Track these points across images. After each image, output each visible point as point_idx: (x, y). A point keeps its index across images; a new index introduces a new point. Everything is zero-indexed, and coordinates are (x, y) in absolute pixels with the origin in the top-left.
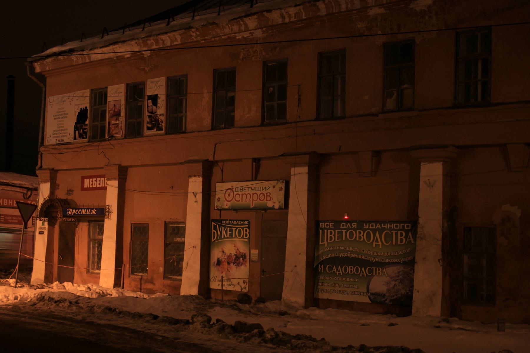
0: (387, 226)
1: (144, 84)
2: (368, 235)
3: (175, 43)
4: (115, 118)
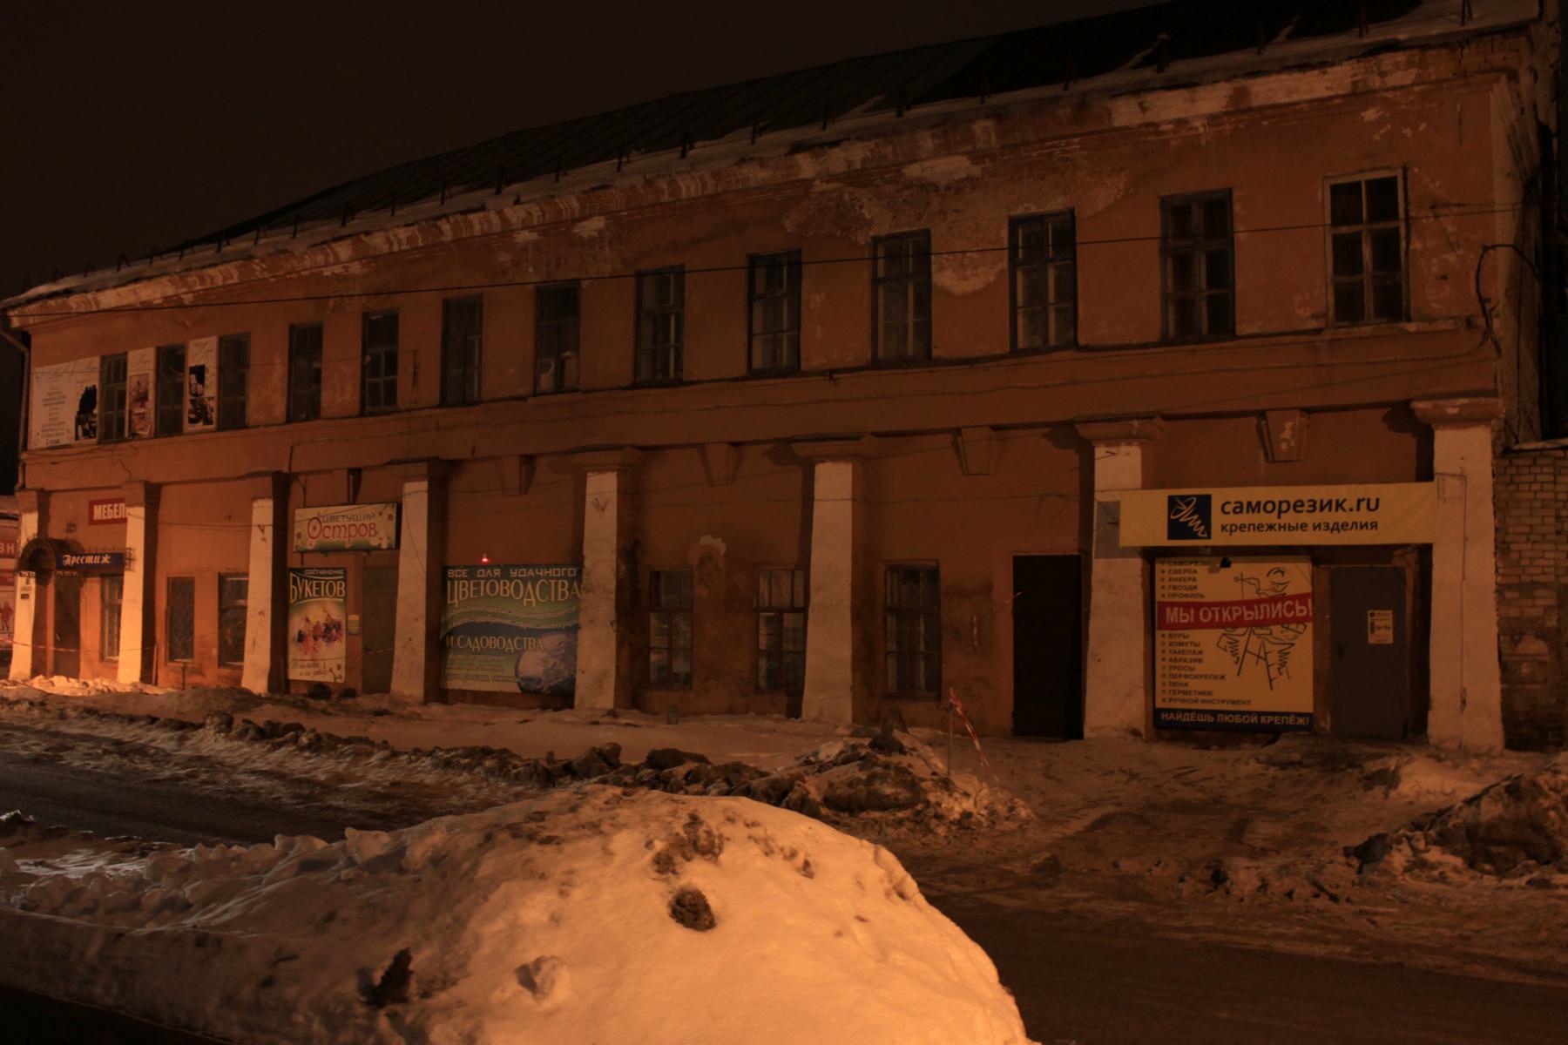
0: (543, 572)
1: (184, 347)
2: (517, 585)
3: (230, 282)
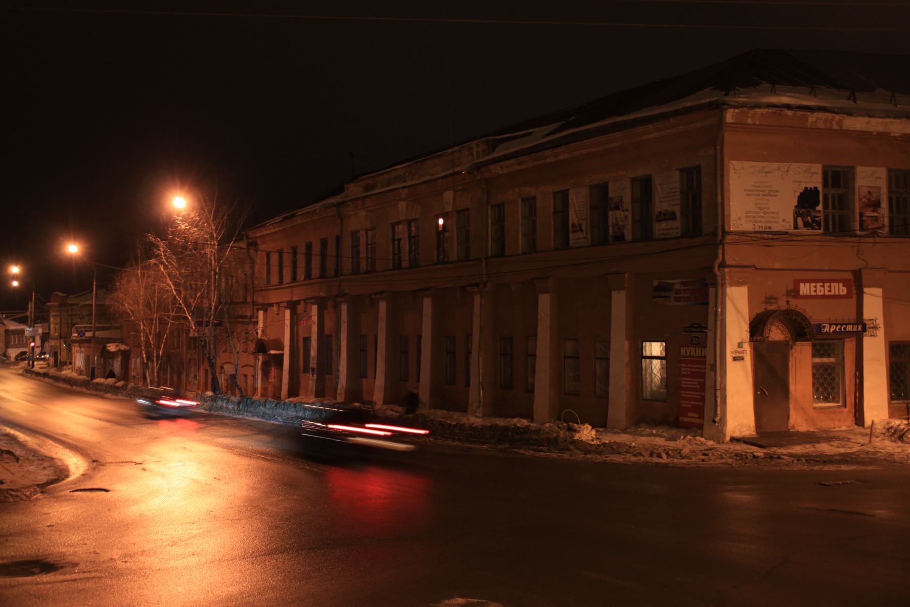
4: (872, 209)
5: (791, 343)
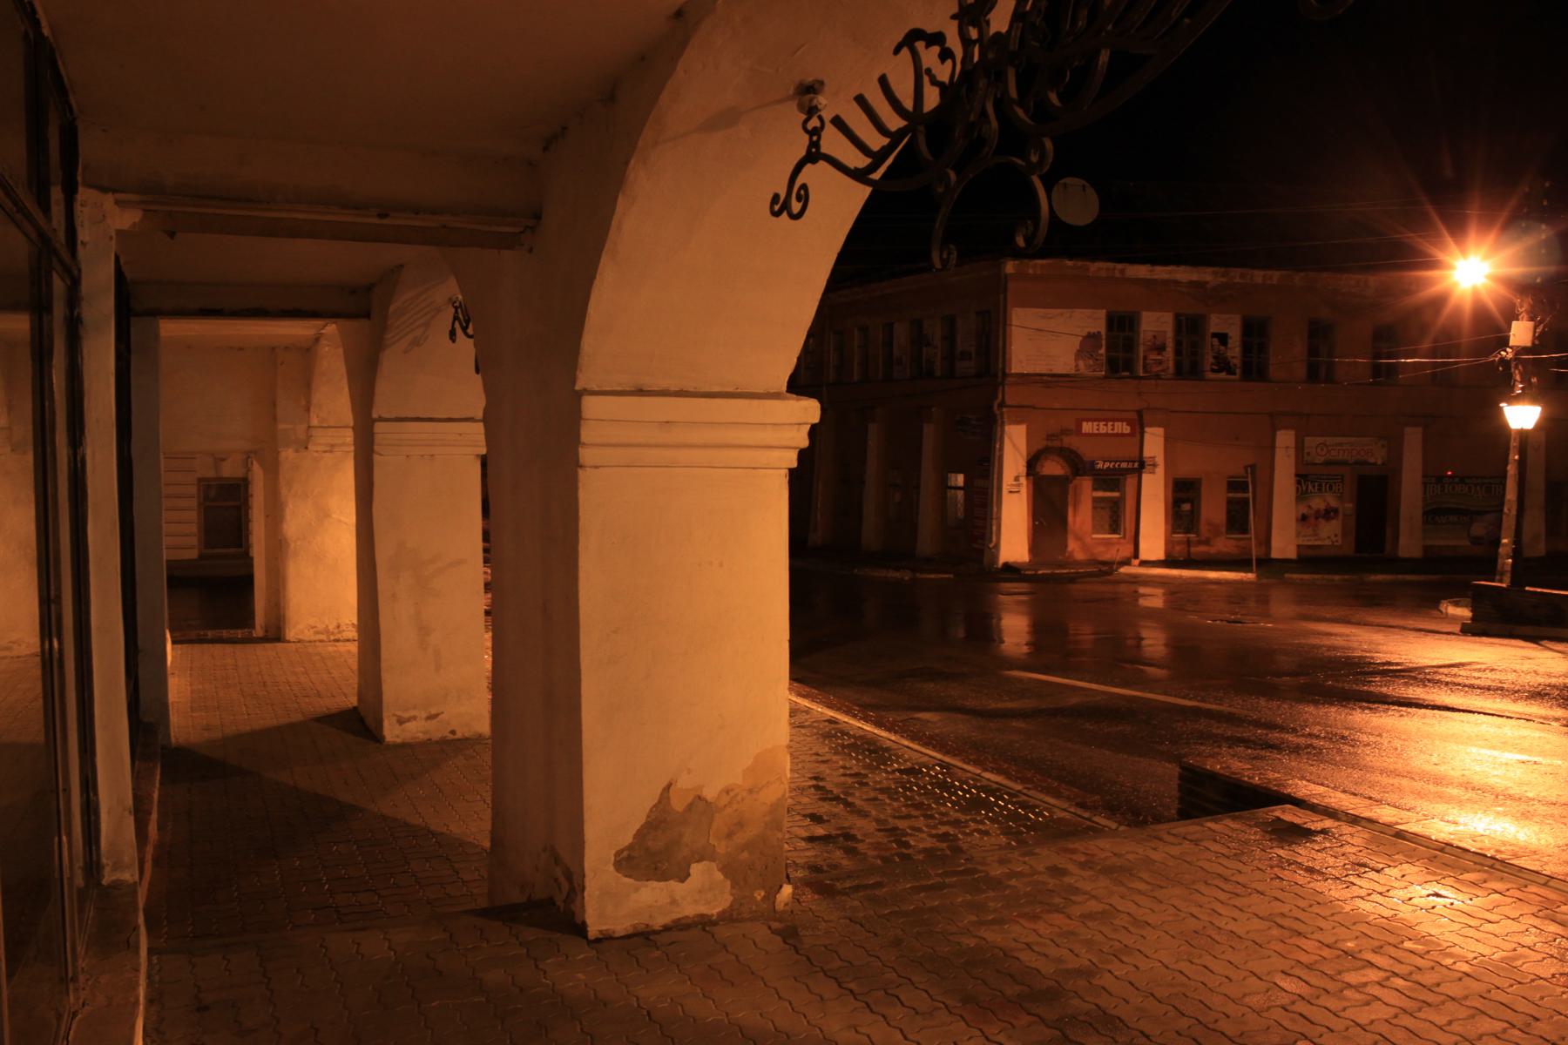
2: (1470, 488)
5: (1071, 477)
